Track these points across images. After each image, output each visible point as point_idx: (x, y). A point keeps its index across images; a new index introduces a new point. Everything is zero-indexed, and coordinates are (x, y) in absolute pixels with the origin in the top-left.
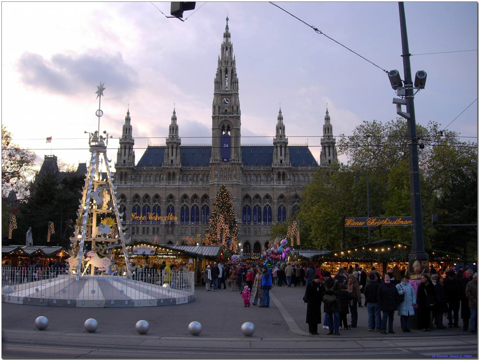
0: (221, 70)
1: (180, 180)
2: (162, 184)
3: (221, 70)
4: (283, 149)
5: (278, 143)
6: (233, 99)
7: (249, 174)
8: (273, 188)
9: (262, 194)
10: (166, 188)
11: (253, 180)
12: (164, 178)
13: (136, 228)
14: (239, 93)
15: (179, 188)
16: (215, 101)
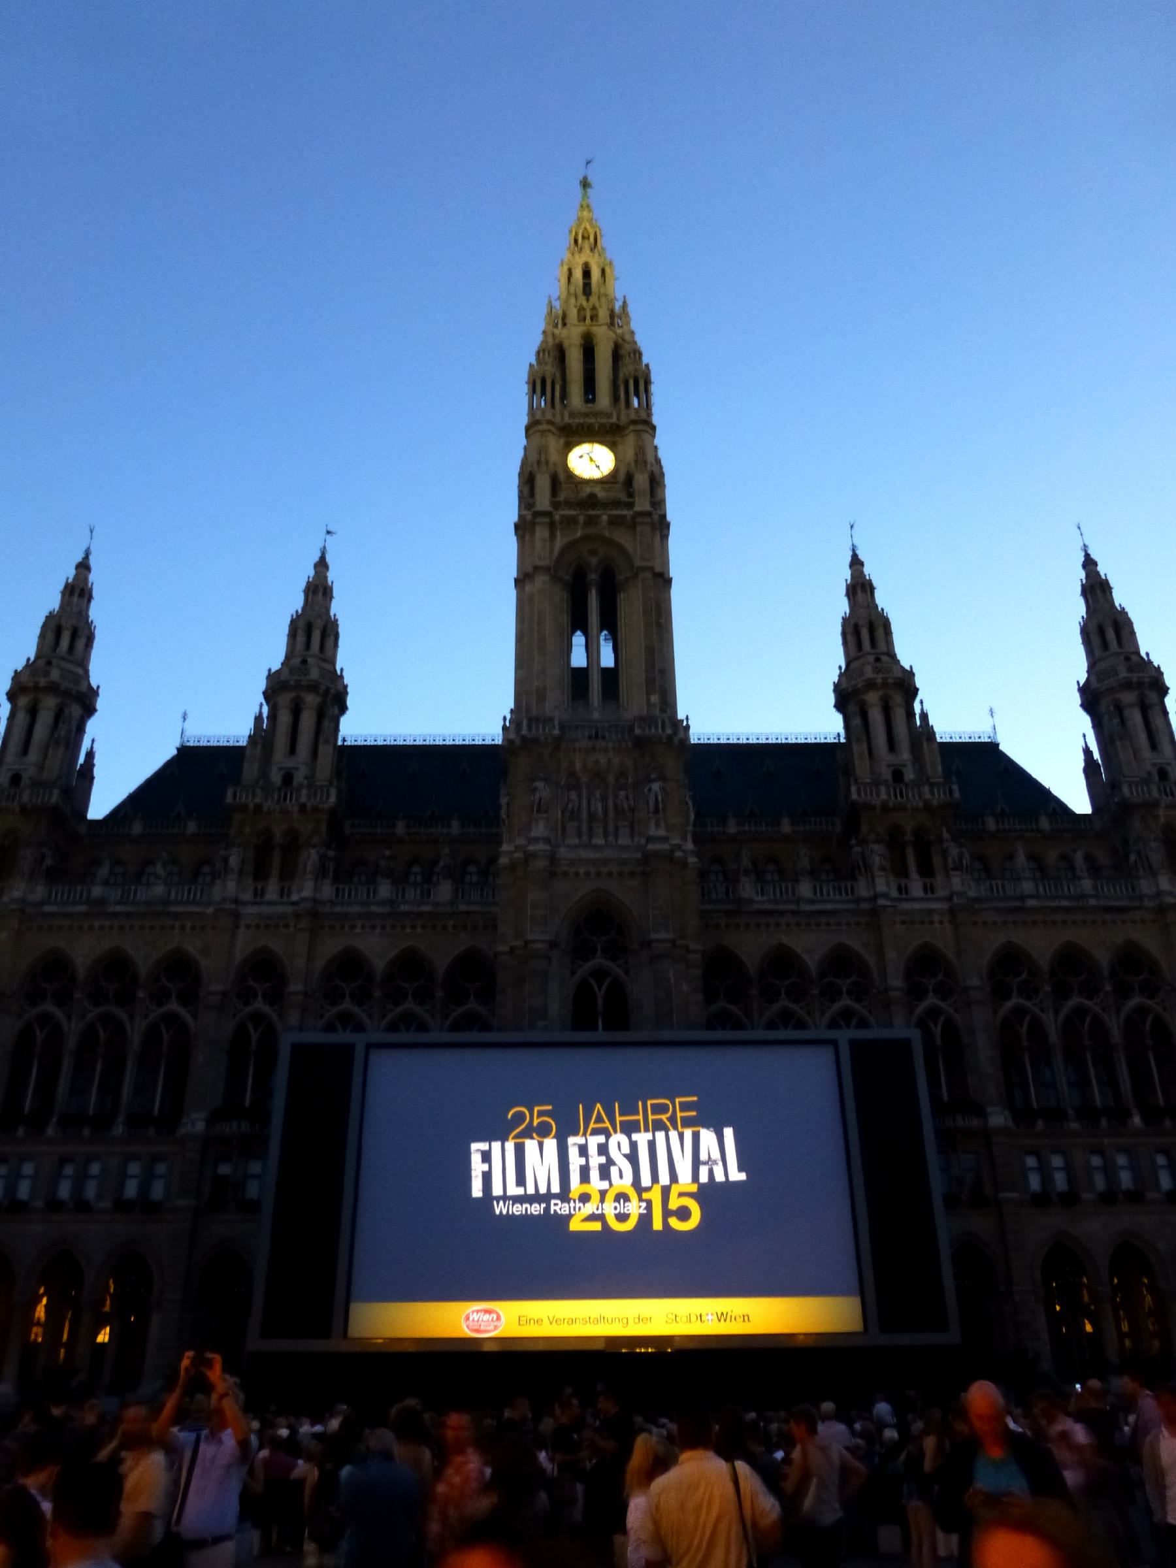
1: (321, 872)
2: (218, 899)
5: (871, 685)
9: (810, 947)
12: (234, 861)
14: (655, 420)
15: (314, 915)
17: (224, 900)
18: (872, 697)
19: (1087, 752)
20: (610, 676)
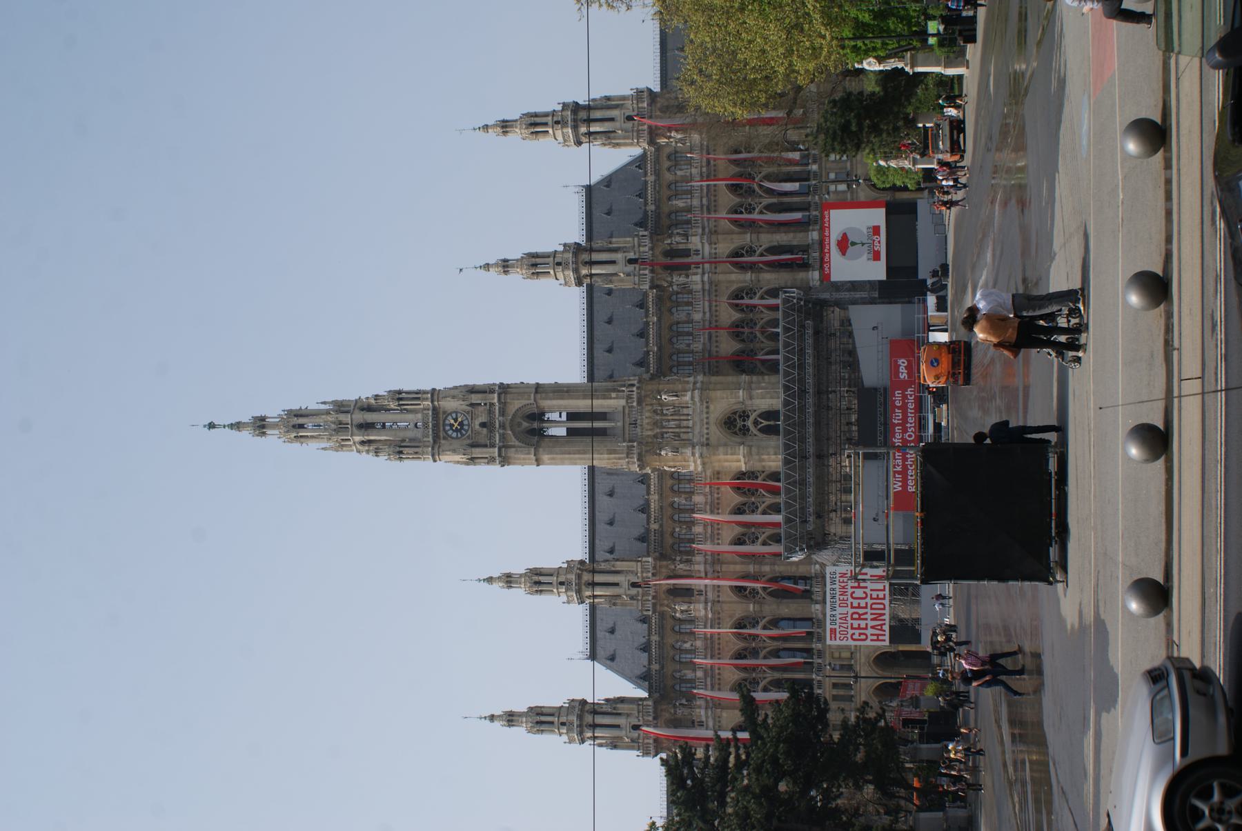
0: (363, 443)
1: (688, 561)
2: (703, 613)
3: (363, 443)
4: (596, 257)
5: (576, 271)
6: (449, 405)
7: (670, 357)
8: (711, 283)
9: (728, 315)
10: (713, 602)
11: (689, 345)
13: (835, 692)
14: (429, 388)
15: (713, 563)
16: (457, 458)
17: (706, 609)
18: (584, 272)
19: (604, 145)
20: (572, 416)
